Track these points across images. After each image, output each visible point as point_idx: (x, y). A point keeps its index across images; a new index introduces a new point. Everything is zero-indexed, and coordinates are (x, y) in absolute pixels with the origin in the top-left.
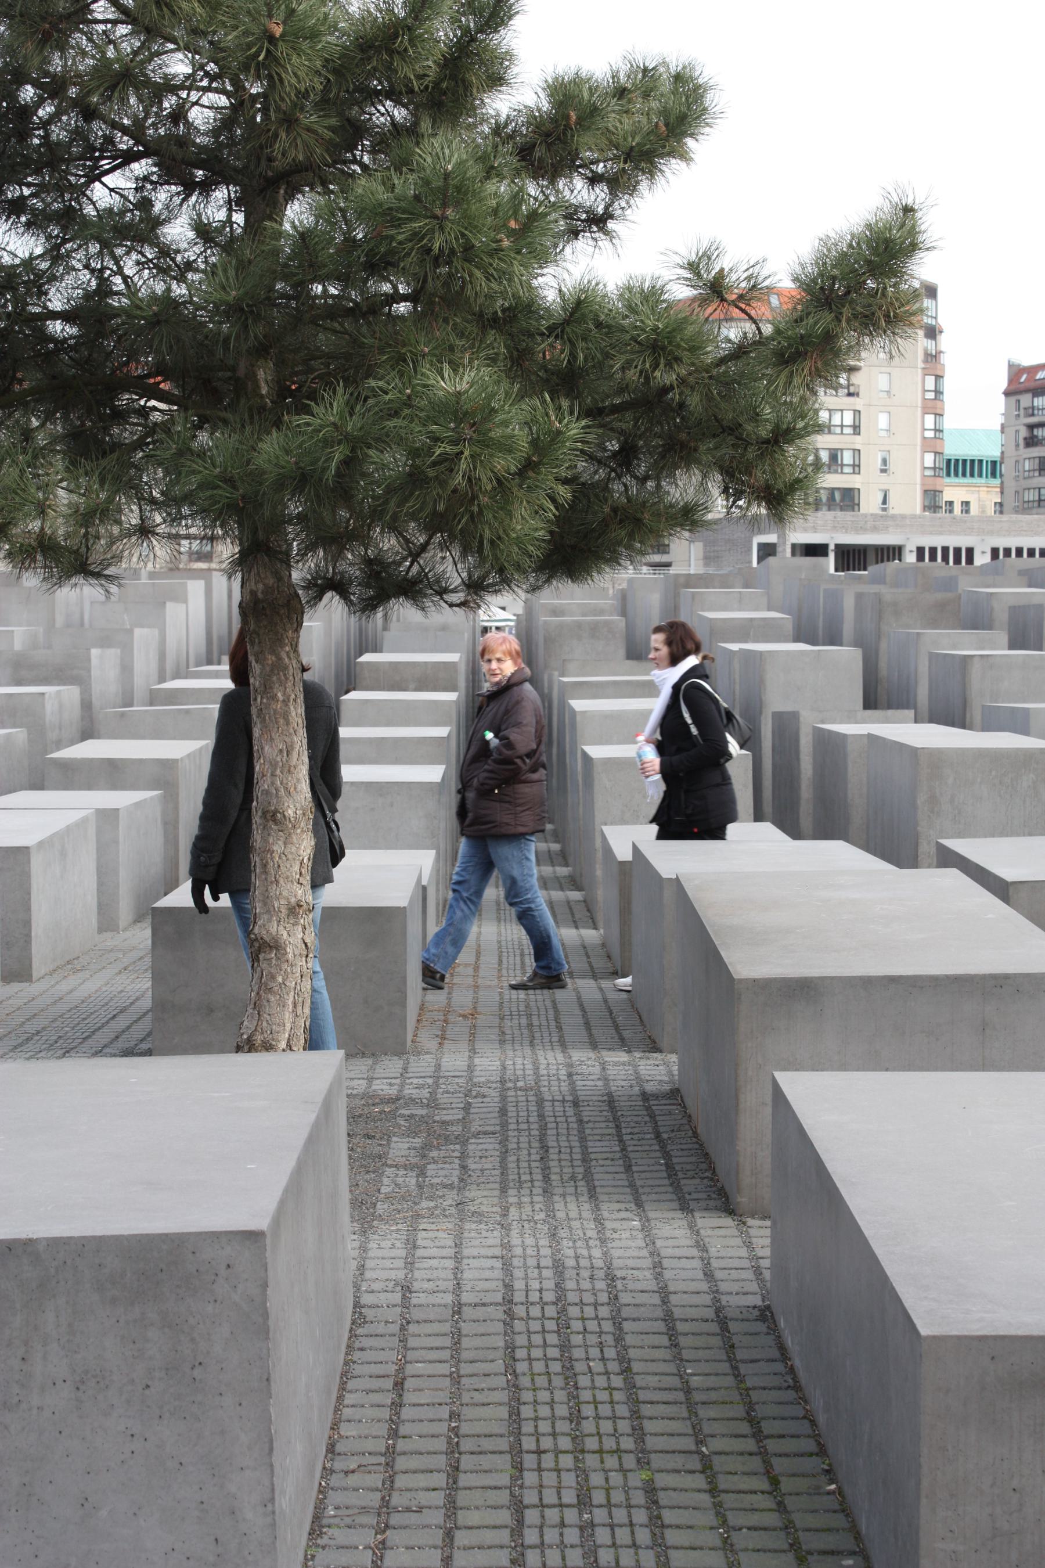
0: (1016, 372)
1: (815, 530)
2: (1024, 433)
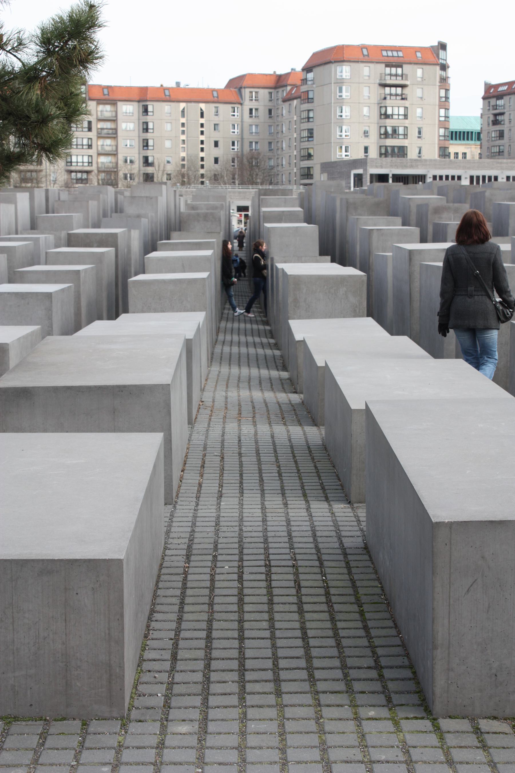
0: (488, 87)
1: (382, 167)
2: (492, 118)
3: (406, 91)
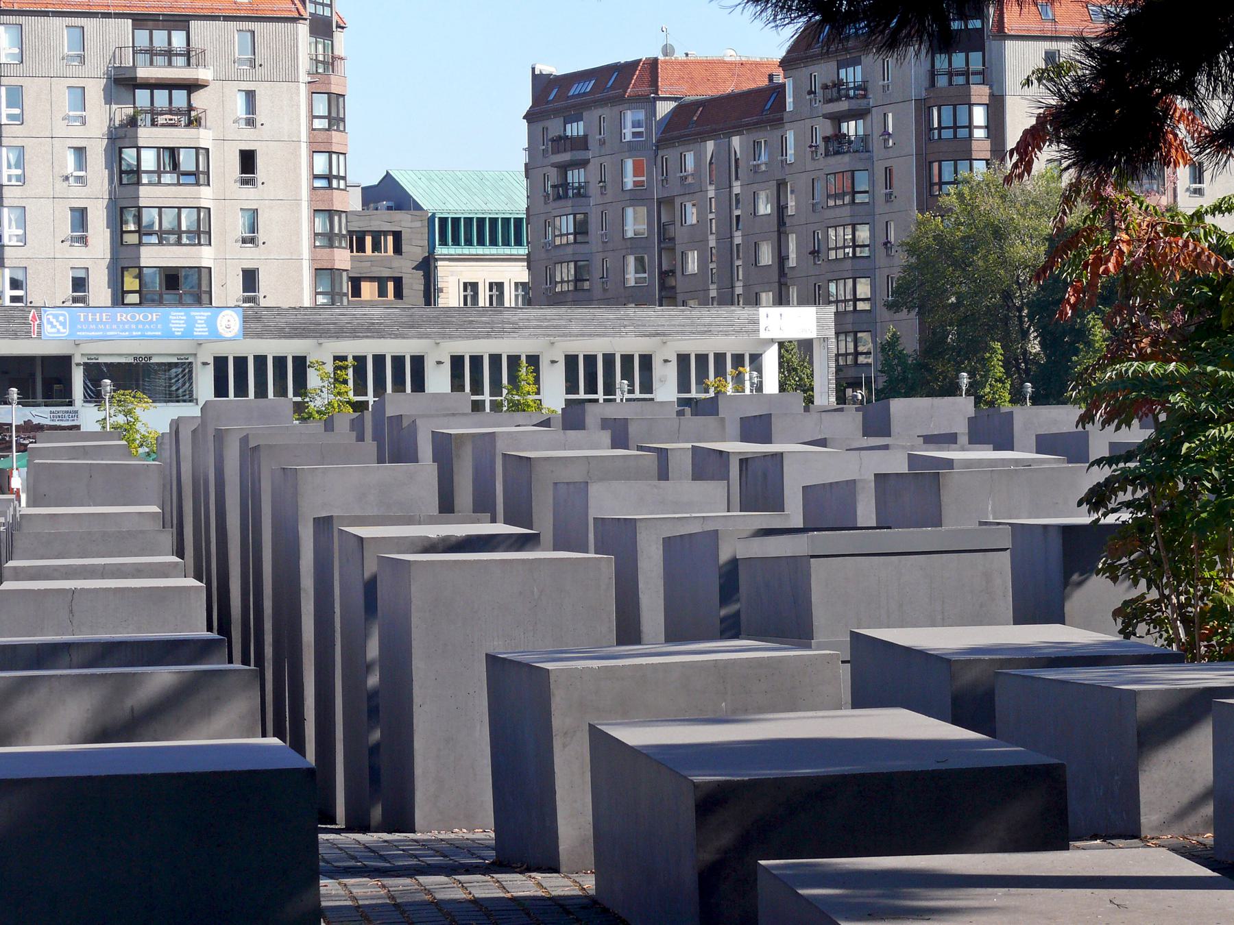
0: (543, 85)
2: (554, 176)
3: (199, 99)
